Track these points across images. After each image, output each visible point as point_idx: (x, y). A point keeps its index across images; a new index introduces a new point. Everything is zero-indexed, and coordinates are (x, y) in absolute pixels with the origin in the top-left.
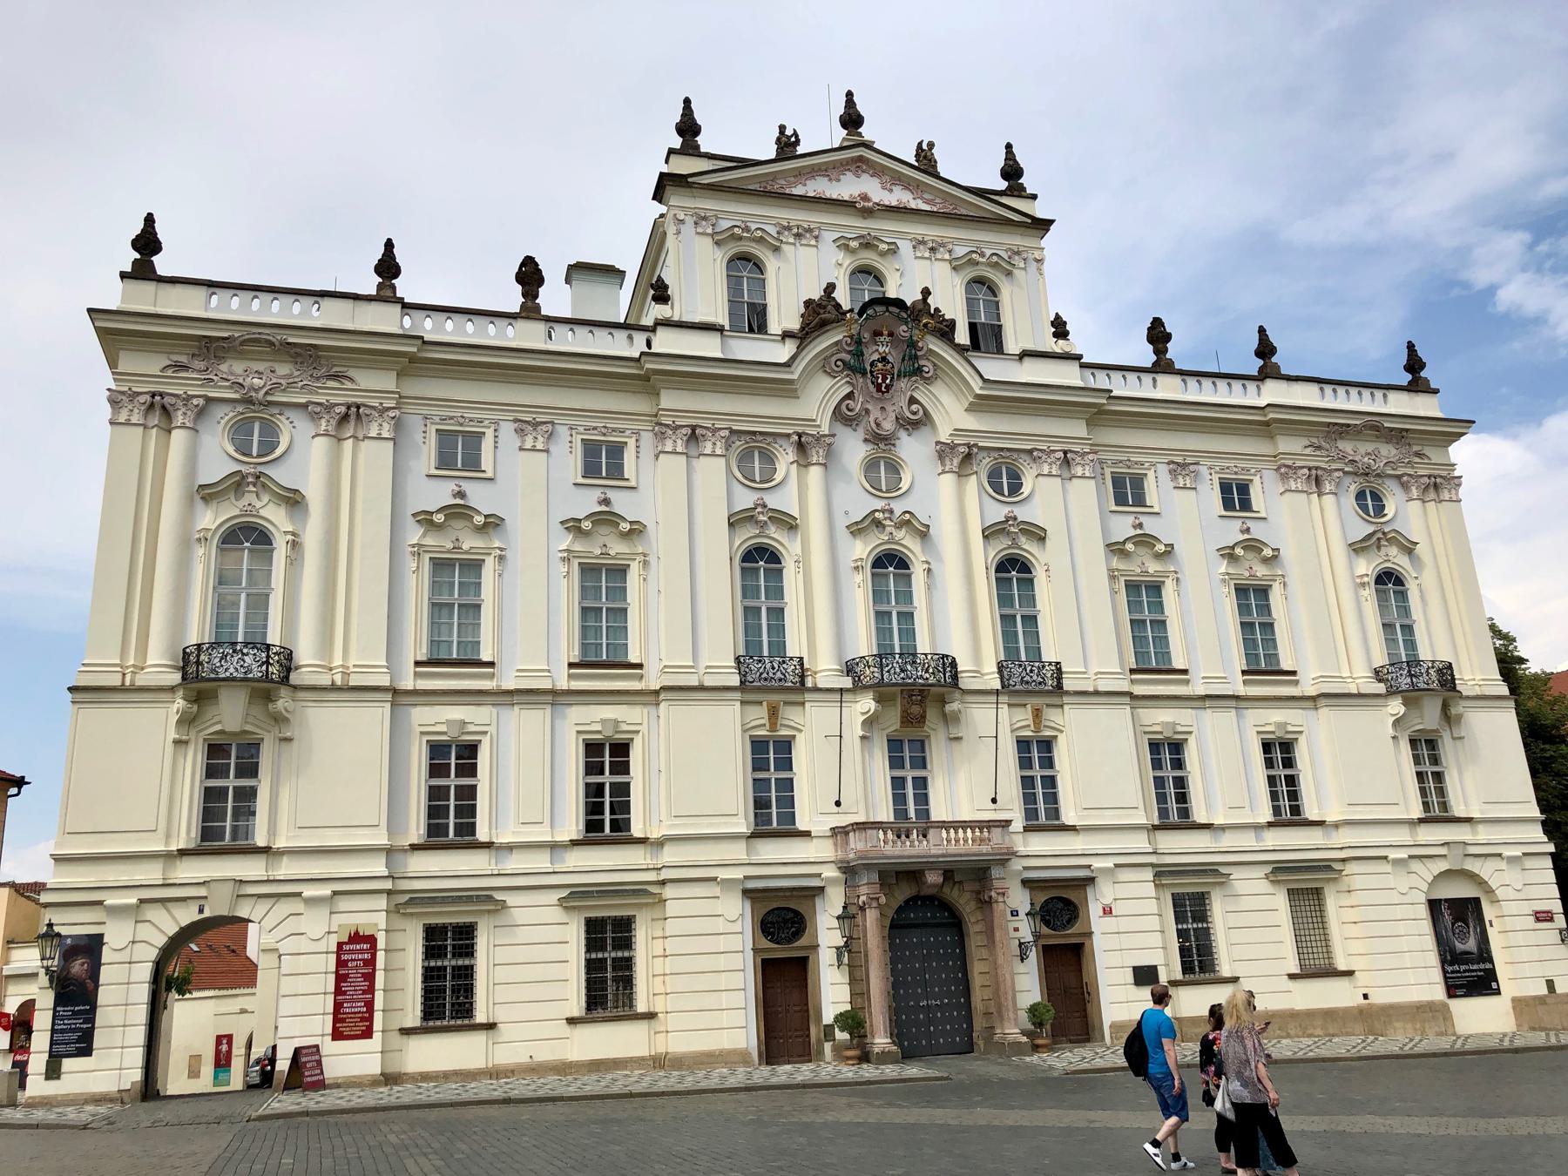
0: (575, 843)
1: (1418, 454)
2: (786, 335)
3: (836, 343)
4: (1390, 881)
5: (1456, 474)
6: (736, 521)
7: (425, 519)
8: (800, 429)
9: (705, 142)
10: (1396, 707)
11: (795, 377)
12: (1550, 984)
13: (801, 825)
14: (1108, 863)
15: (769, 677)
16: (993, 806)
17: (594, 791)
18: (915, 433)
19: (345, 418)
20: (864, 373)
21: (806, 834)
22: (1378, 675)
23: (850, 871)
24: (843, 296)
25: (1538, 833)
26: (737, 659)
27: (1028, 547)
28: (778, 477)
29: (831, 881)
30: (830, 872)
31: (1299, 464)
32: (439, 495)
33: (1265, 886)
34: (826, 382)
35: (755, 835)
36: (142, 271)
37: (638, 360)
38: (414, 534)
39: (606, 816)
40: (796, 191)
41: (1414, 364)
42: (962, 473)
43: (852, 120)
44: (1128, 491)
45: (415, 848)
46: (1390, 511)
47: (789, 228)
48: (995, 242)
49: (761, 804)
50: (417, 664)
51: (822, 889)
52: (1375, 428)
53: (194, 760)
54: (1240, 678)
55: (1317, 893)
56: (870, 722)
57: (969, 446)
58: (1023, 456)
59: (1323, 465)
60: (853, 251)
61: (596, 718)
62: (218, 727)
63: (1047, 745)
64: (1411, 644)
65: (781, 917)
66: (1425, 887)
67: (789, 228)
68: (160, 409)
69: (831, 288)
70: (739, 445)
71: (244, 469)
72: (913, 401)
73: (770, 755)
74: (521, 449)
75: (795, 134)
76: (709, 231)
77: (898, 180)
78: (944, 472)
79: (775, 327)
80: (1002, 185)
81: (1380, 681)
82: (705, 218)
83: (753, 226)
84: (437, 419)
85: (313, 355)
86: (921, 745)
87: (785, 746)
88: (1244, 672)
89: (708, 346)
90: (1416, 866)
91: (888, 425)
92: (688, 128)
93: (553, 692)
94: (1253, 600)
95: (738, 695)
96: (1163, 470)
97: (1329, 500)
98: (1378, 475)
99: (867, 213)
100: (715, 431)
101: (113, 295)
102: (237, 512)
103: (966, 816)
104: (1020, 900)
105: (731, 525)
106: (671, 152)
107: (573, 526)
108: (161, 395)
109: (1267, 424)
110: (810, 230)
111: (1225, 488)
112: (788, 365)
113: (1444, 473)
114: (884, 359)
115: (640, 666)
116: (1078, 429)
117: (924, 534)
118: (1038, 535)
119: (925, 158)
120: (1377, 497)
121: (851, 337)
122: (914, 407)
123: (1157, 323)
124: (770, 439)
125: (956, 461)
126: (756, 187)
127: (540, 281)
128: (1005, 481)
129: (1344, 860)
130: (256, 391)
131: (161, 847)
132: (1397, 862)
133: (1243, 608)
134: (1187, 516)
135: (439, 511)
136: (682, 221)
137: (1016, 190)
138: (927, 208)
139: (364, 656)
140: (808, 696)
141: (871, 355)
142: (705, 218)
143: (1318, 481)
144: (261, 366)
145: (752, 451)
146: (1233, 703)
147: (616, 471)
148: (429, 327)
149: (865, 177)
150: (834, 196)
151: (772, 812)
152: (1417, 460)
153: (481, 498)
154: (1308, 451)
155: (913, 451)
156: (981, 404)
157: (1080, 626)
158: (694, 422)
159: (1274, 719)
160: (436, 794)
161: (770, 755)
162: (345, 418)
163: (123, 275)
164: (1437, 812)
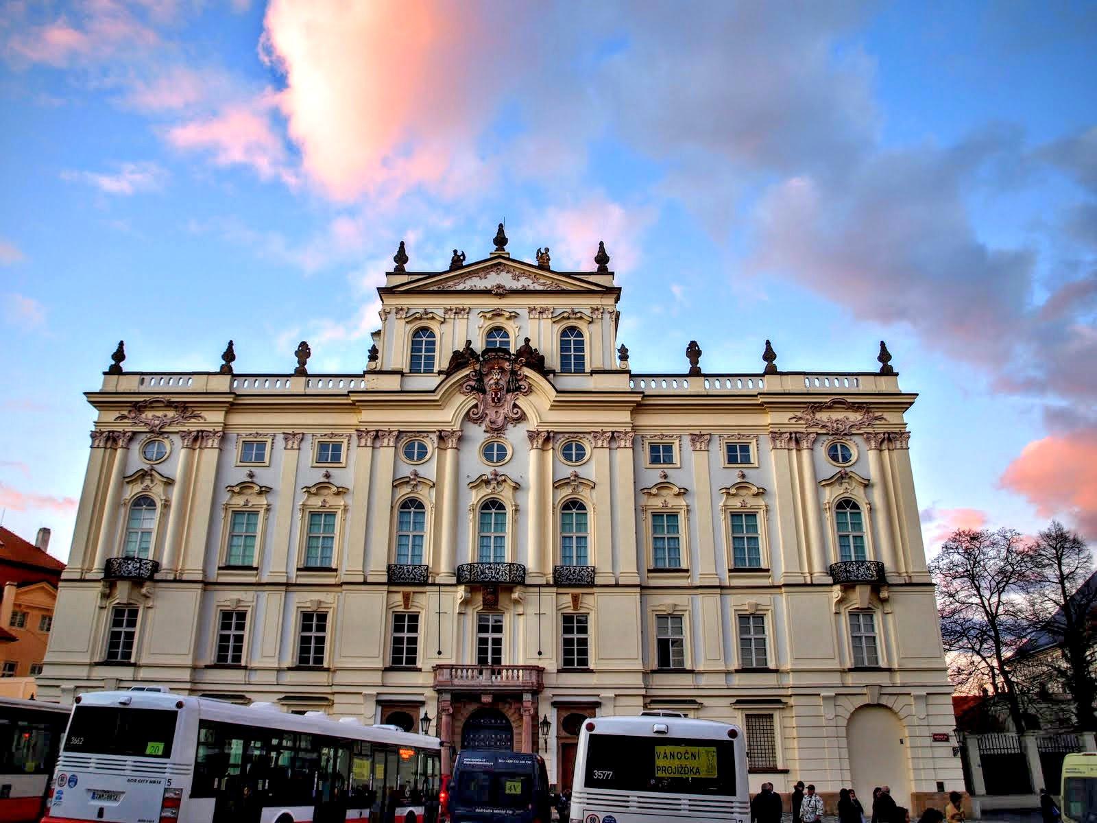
0: (290, 669)
1: (877, 418)
2: (440, 373)
3: (466, 376)
5: (907, 430)
6: (397, 484)
7: (231, 489)
8: (440, 428)
9: (408, 267)
10: (837, 592)
11: (437, 398)
13: (419, 665)
14: (611, 694)
15: (405, 577)
16: (538, 657)
17: (305, 640)
18: (518, 425)
19: (196, 439)
20: (484, 392)
21: (420, 670)
22: (831, 571)
23: (439, 692)
24: (479, 346)
26: (389, 567)
27: (585, 495)
28: (427, 457)
29: (431, 698)
30: (430, 693)
31: (782, 430)
32: (237, 475)
33: (729, 712)
35: (386, 670)
36: (115, 370)
37: (347, 395)
38: (225, 497)
39: (311, 653)
40: (460, 287)
41: (884, 356)
42: (543, 449)
43: (501, 241)
44: (661, 454)
45: (208, 667)
46: (854, 459)
47: (451, 310)
48: (584, 304)
49: (397, 651)
50: (220, 568)
51: (423, 703)
52: (839, 402)
53: (107, 616)
54: (727, 574)
55: (771, 716)
56: (466, 603)
57: (548, 433)
58: (587, 436)
59: (803, 430)
60: (490, 319)
61: (307, 599)
62: (117, 601)
64: (860, 548)
66: (848, 716)
67: (451, 310)
69: (469, 342)
70: (404, 440)
71: (146, 467)
72: (515, 406)
73: (405, 623)
74: (285, 449)
75: (463, 254)
76: (404, 316)
77: (524, 273)
78: (532, 448)
79: (436, 369)
80: (594, 267)
81: (832, 575)
82: (402, 309)
83: (430, 311)
84: (244, 435)
85: (185, 407)
87: (414, 618)
88: (730, 571)
89: (393, 383)
90: (842, 700)
91: (500, 420)
92: (401, 258)
93: (287, 585)
94: (743, 522)
95: (386, 588)
96: (687, 441)
97: (805, 454)
98: (845, 434)
99: (500, 296)
100: (391, 432)
101: (97, 384)
102: (140, 490)
103: (521, 663)
104: (549, 713)
105: (394, 487)
106: (388, 274)
107: (307, 490)
108: (113, 432)
109: (762, 404)
110: (464, 310)
111: (731, 449)
112: (433, 392)
113: (897, 430)
114: (497, 383)
115: (336, 570)
116: (624, 416)
117: (517, 487)
121: (475, 371)
122: (515, 411)
123: (693, 344)
124: (425, 435)
125: (540, 442)
126: (435, 288)
127: (309, 355)
128: (573, 450)
129: (790, 696)
130: (156, 427)
131: (88, 661)
132: (825, 698)
133: (736, 527)
134: (700, 472)
135: (237, 486)
136: (389, 313)
137: (603, 270)
138: (541, 288)
139: (193, 565)
140: (428, 588)
141: (490, 381)
142: (402, 309)
143: (797, 442)
144: (160, 414)
145: (411, 445)
146: (718, 591)
147: (336, 458)
148: (246, 387)
149: (503, 274)
150: (482, 288)
151: (403, 656)
152: (878, 422)
153: (264, 477)
154: (793, 421)
155: (515, 436)
156: (557, 406)
157: (613, 544)
158: (377, 428)
159: (746, 601)
160: (224, 639)
161: (405, 623)
162: (196, 439)
163: (105, 373)
164: (866, 664)
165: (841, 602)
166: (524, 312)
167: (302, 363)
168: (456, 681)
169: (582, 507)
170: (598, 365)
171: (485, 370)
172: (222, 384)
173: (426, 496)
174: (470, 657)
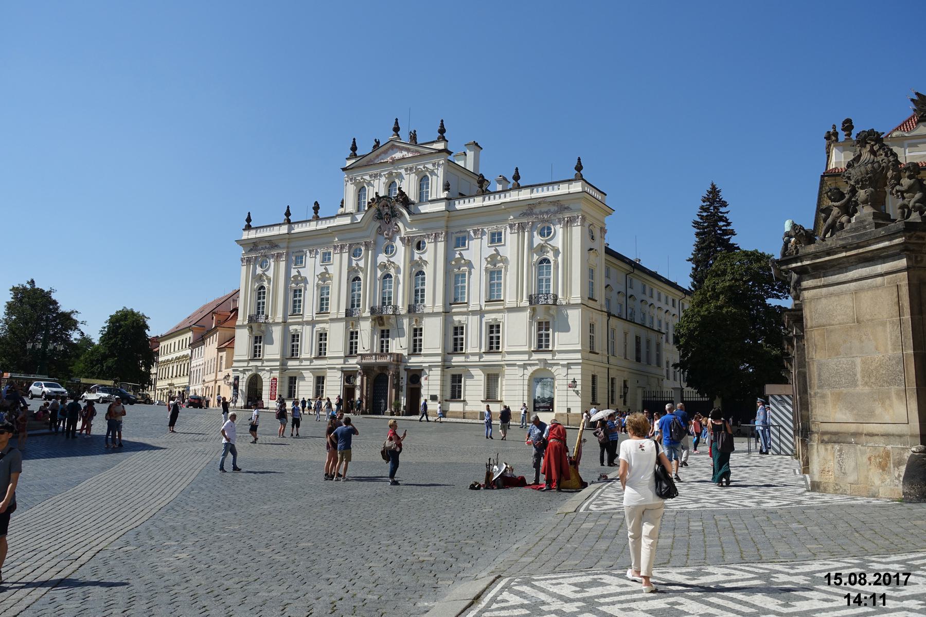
4: (517, 372)
6: (351, 270)
12: (569, 410)
14: (427, 365)
25: (579, 356)
34: (374, 223)
41: (579, 168)
43: (396, 129)
63: (421, 330)
64: (548, 286)
65: (349, 376)
68: (249, 261)
85: (272, 243)
86: (388, 331)
89: (347, 221)
92: (354, 148)
94: (494, 276)
104: (404, 375)
118: (426, 262)
119: (413, 137)
120: (549, 229)
138: (410, 155)
159: (489, 318)
164: (544, 348)
165: (532, 317)
166: (403, 171)
167: (316, 213)
168: (364, 361)
169: (424, 274)
170: (434, 197)
171: (381, 208)
172: (284, 230)
173: (361, 275)
174: (376, 350)
